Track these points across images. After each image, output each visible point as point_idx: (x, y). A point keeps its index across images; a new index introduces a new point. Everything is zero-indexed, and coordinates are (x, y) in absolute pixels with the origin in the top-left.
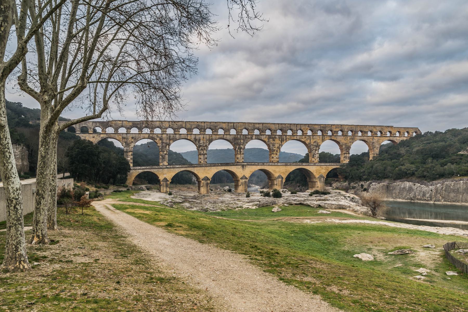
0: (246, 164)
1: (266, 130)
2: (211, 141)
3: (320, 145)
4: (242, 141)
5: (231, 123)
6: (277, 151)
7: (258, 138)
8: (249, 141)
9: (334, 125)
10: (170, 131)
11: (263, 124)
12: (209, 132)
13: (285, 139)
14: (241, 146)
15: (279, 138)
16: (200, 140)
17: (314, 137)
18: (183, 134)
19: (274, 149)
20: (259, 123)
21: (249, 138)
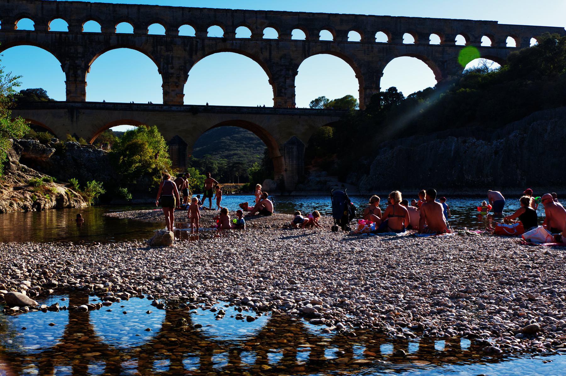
3: (298, 66)
4: (80, 49)
6: (178, 78)
7: (124, 42)
13: (199, 46)
17: (281, 43)
19: (171, 71)
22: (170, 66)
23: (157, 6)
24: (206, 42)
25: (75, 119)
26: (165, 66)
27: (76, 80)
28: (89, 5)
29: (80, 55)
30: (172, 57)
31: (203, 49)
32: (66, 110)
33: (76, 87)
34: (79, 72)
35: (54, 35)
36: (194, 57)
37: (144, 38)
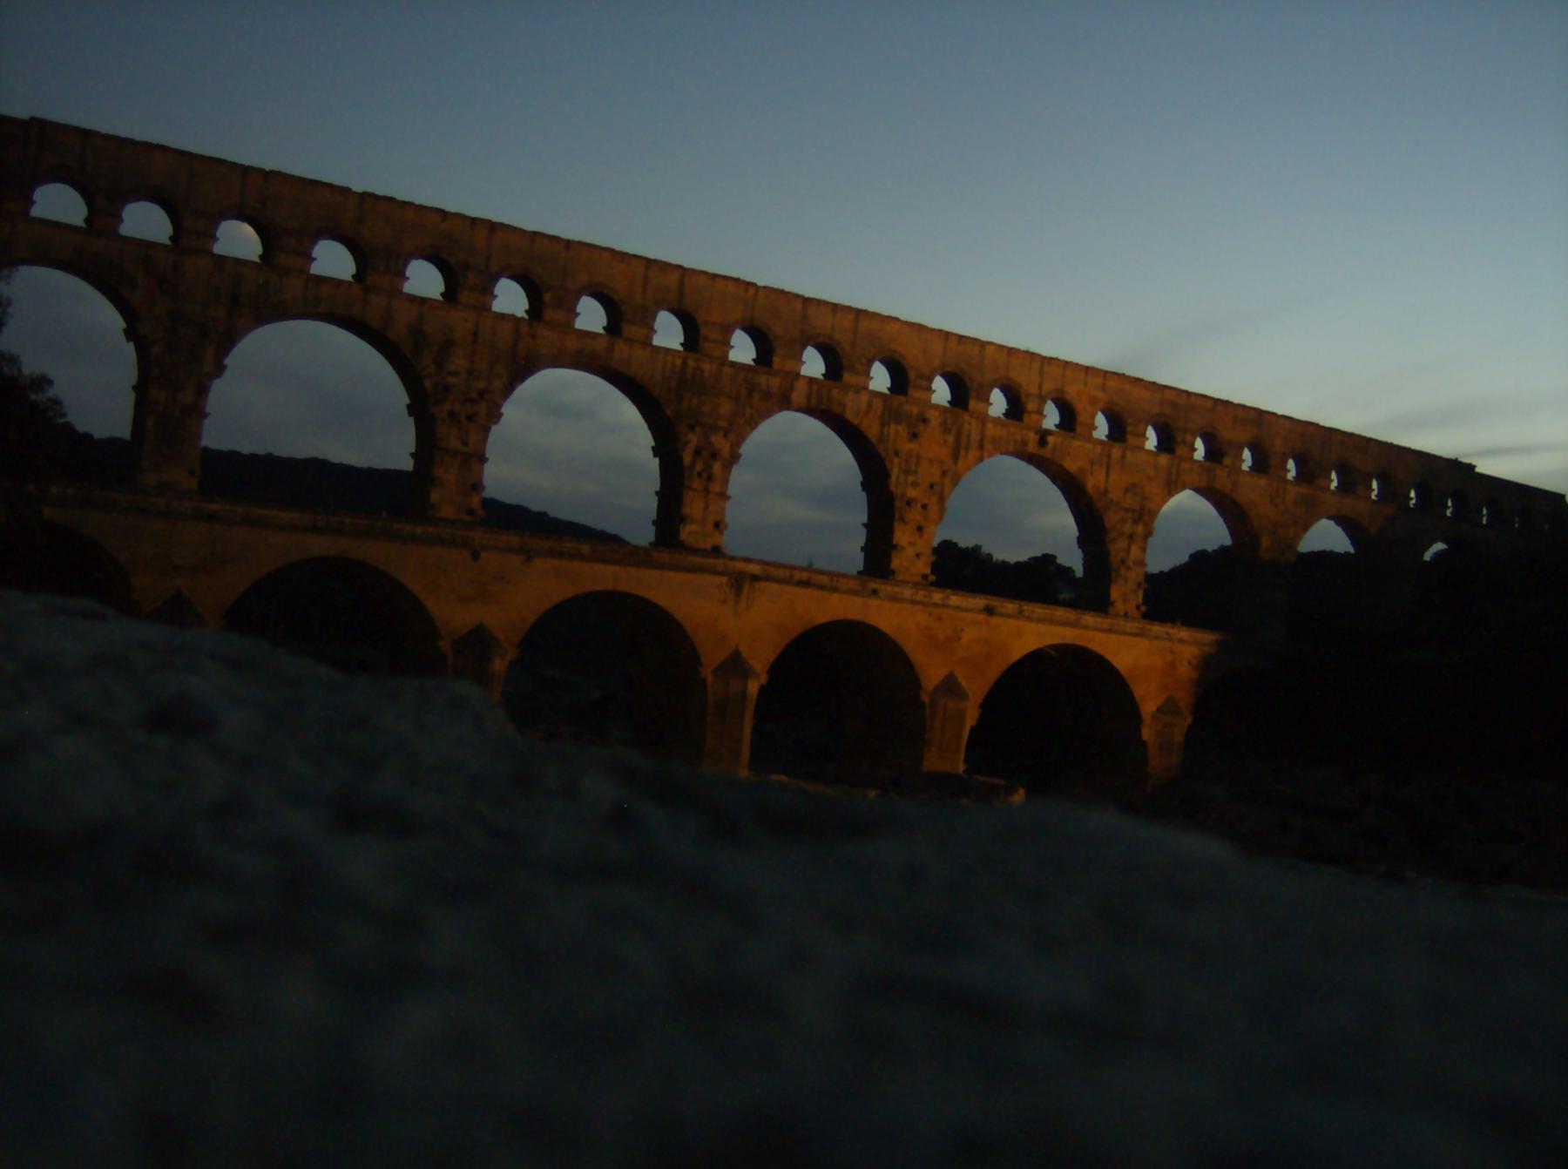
0: (755, 569)
1: (870, 363)
2: (523, 369)
4: (726, 408)
5: (665, 267)
8: (768, 414)
9: (1227, 403)
10: (239, 240)
11: (859, 313)
12: (510, 299)
13: (975, 437)
14: (717, 440)
15: (945, 428)
16: (448, 345)
18: (339, 283)
19: (911, 493)
20: (835, 307)
21: (768, 395)
22: (911, 479)
23: (897, 319)
24: (991, 430)
25: (743, 605)
26: (902, 478)
27: (707, 491)
28: (752, 291)
29: (722, 423)
30: (918, 457)
31: (981, 447)
32: (725, 579)
33: (706, 507)
34: (717, 468)
35: (670, 358)
36: (960, 463)
37: (864, 398)
